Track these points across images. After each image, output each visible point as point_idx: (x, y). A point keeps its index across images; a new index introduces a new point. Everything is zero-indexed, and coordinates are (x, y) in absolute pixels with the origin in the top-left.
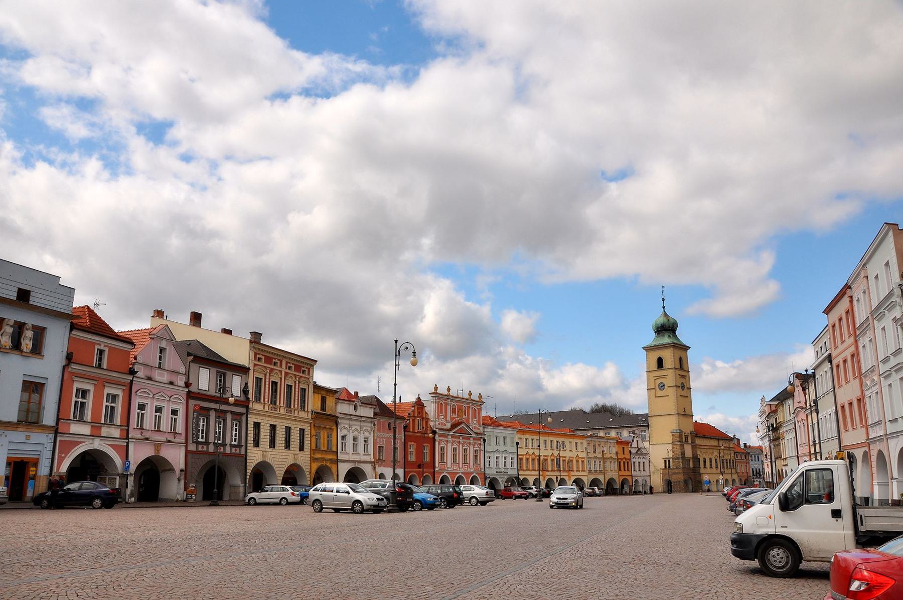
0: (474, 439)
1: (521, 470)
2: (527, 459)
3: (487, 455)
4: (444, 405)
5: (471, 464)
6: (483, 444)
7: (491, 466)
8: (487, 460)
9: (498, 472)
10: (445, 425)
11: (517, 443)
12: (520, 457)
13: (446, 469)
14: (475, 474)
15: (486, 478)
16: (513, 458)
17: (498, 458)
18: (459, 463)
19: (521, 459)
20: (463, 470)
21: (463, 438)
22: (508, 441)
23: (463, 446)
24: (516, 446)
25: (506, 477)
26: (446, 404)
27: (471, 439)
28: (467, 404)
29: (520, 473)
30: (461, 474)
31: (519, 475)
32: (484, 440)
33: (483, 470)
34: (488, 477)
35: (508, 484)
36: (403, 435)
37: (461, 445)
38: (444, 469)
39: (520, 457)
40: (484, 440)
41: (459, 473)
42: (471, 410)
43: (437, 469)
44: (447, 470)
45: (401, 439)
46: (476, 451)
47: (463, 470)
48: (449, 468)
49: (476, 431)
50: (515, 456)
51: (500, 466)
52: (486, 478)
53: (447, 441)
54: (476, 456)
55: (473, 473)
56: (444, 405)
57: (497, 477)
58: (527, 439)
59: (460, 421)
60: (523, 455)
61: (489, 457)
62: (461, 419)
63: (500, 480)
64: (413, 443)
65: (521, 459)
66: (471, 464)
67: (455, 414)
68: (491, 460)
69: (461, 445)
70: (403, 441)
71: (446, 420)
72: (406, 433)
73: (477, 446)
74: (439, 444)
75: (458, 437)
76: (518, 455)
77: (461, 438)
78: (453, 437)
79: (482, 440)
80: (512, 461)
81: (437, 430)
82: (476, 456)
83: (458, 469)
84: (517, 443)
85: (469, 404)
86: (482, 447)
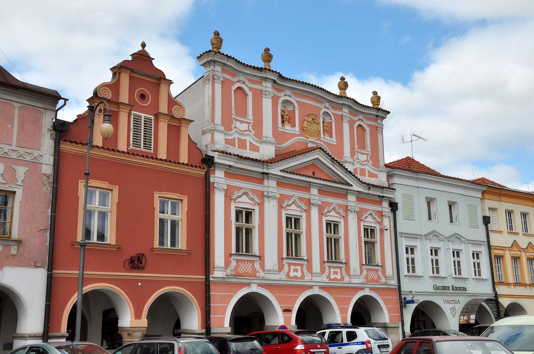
0: (361, 197)
1: (502, 283)
2: (516, 259)
3: (403, 243)
4: (250, 94)
5: (355, 263)
6: (391, 215)
7: (418, 272)
8: (403, 256)
9: (437, 288)
10: (255, 148)
11: (486, 220)
12: (495, 252)
13: (261, 274)
14: (367, 292)
15: (403, 303)
16: (476, 255)
17: (435, 251)
18: (309, 261)
19: (499, 258)
20: (325, 279)
21: (322, 191)
22: (461, 211)
23: (321, 214)
24: (482, 227)
25: (464, 300)
26: (258, 95)
27: (352, 198)
28: (334, 108)
29: (501, 290)
30: (316, 291)
31: (496, 296)
32: (394, 206)
33: (394, 282)
34: (409, 298)
35: (469, 319)
36: (51, 151)
37: (315, 212)
38: (254, 274)
39: (495, 252)
40: (394, 206)
41: (311, 287)
42: (346, 126)
43: (217, 274)
44: (263, 279)
45: (35, 164)
46: (369, 232)
47: (324, 278)
48: (270, 272)
49: (367, 179)
50: (483, 250)
51: (442, 273)
52: (403, 303)
53: (262, 195)
54: (370, 245)
55: (363, 289)
56: (250, 94)
57: (439, 300)
58: (509, 213)
59: (310, 145)
60: (503, 248)
61: (411, 250)
62: (311, 143)
63: (446, 308)
64: (105, 185)
65: (499, 258)
66: (355, 263)
67: (294, 126)
68: (418, 255)
69: (315, 212)
70: (48, 169)
71: (259, 134)
72: (66, 147)
73: (370, 219)
74: (228, 198)
75: (307, 187)
76: (490, 247)
77: (314, 191)
78: (281, 183)
79: (386, 204)
80: (476, 261)
81: (215, 155)
82: (370, 245)
83: (308, 277)
84: (486, 220)
85: (341, 109)
86: (387, 223)
